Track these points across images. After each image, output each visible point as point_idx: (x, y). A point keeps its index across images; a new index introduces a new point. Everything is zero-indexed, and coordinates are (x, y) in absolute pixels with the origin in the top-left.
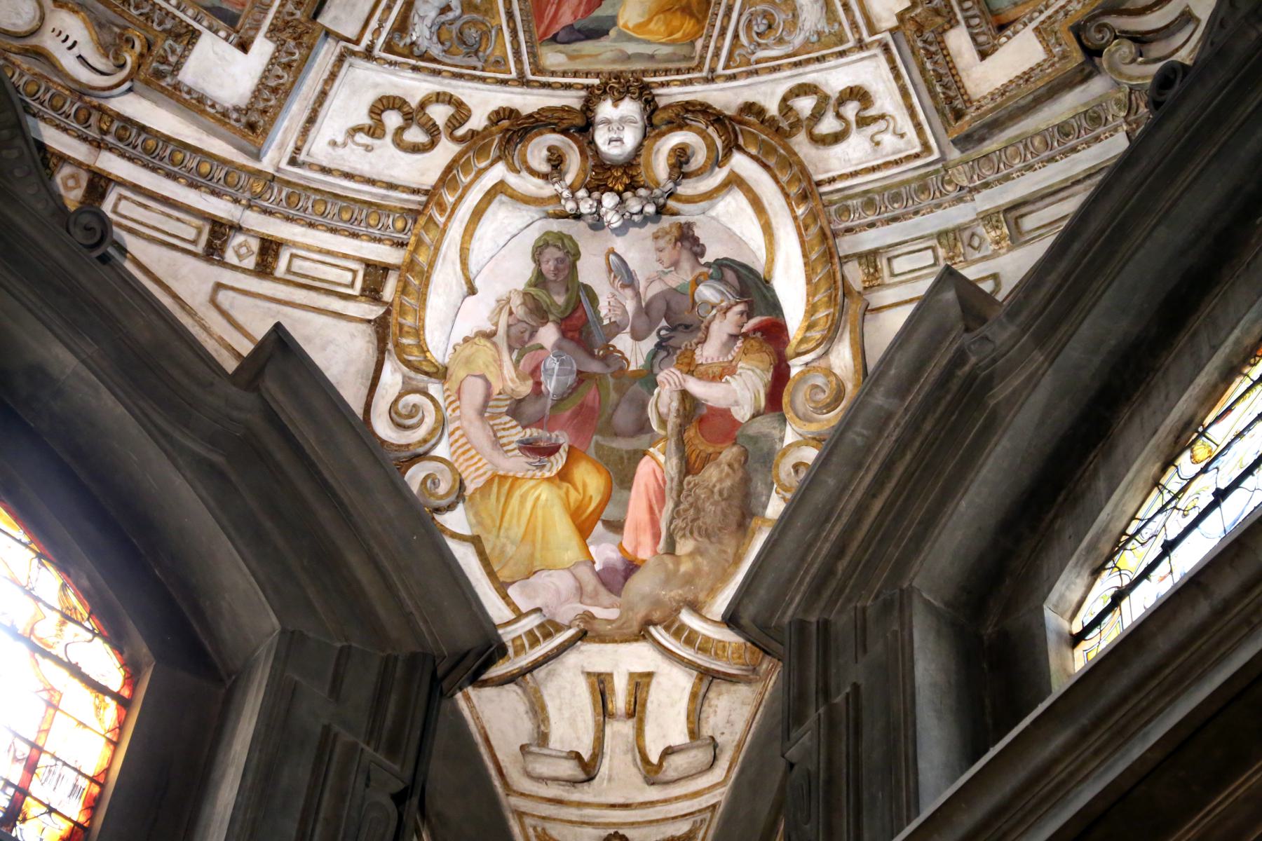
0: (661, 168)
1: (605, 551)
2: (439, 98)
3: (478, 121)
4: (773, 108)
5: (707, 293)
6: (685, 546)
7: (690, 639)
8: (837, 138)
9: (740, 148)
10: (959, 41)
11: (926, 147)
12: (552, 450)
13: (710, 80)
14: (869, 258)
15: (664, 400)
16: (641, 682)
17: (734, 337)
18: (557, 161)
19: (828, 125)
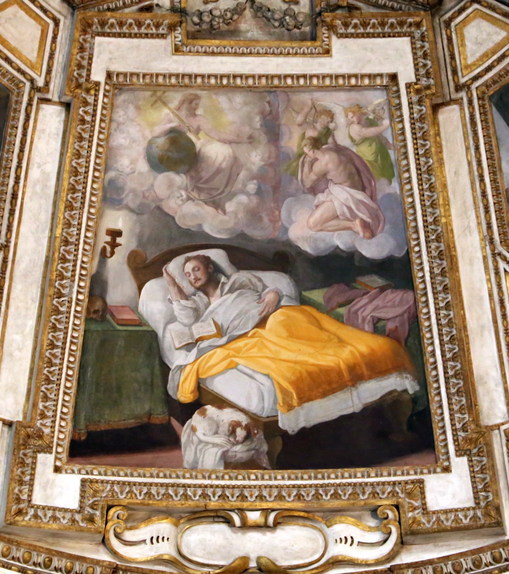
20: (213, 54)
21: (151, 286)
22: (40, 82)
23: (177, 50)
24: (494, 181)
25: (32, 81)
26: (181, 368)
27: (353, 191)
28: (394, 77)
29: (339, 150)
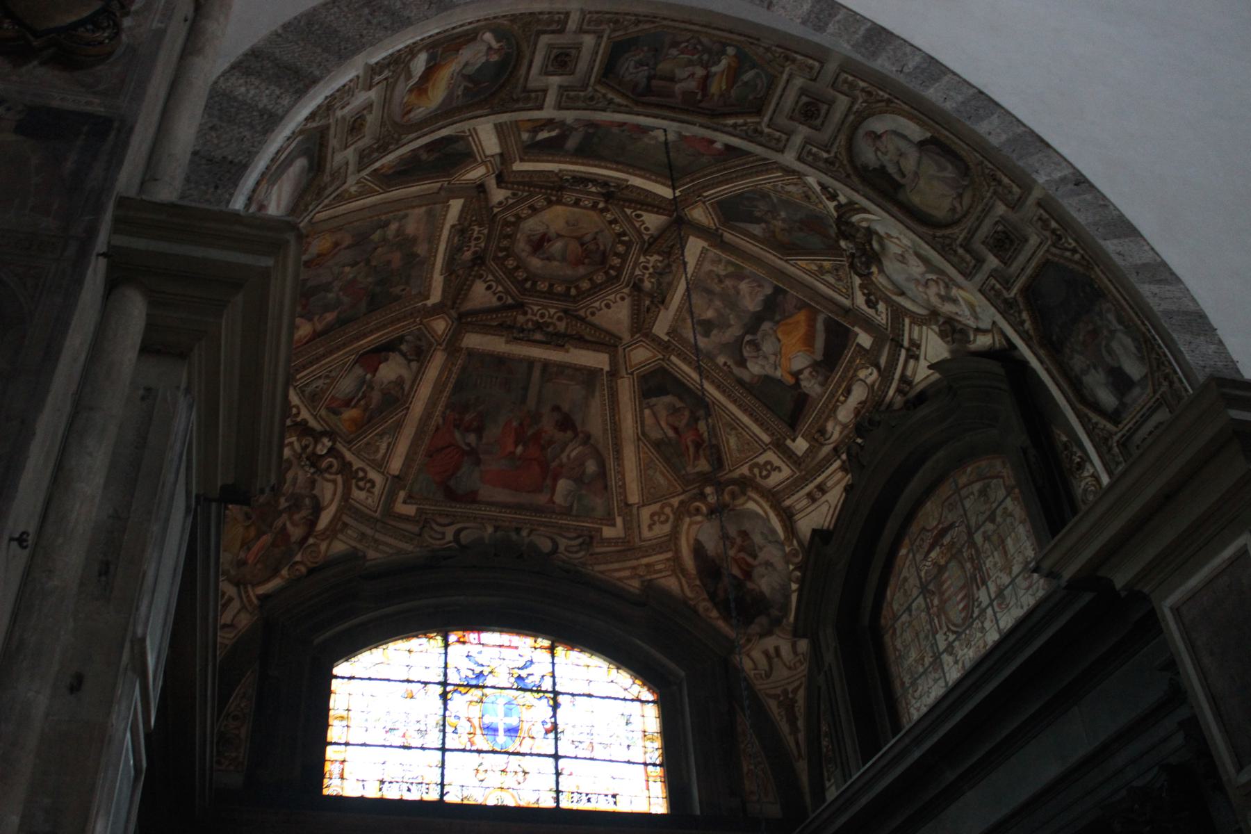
0: (324, 464)
1: (242, 555)
2: (297, 407)
3: (299, 419)
4: (355, 468)
5: (307, 501)
6: (259, 566)
7: (248, 596)
8: (361, 489)
9: (342, 475)
10: (402, 494)
11: (376, 512)
12: (250, 518)
13: (349, 450)
14: (345, 525)
15: (279, 523)
16: (230, 600)
17: (304, 517)
18: (307, 446)
19: (361, 484)
20: (672, 299)
21: (749, 365)
22: (661, 356)
23: (667, 309)
24: (758, 242)
25: (659, 359)
26: (782, 376)
27: (744, 282)
28: (703, 247)
29: (726, 276)
